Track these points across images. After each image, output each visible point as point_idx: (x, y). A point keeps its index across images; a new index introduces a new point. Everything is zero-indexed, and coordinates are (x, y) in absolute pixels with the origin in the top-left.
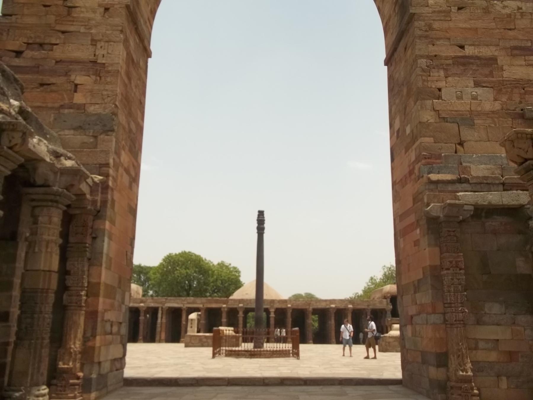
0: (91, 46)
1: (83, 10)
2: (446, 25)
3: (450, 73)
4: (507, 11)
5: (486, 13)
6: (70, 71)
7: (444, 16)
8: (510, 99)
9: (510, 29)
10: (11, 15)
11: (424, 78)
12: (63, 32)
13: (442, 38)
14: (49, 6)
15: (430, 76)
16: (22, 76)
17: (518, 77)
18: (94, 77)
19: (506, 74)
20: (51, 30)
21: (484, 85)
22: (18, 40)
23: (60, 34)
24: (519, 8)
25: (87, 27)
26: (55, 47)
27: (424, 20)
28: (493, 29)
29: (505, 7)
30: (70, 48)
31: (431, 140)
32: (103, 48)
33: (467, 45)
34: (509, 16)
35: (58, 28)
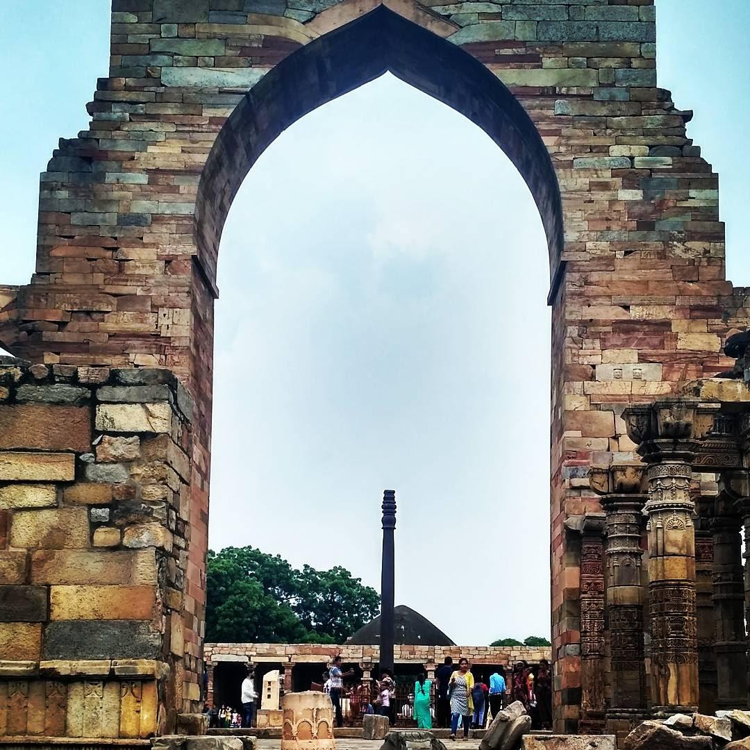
0: (151, 315)
1: (137, 264)
2: (606, 276)
3: (607, 344)
4: (690, 255)
5: (661, 258)
6: (127, 348)
7: (604, 264)
8: (683, 379)
9: (692, 282)
10: (49, 274)
11: (574, 351)
12: (115, 295)
13: (601, 296)
14: (95, 260)
15: (582, 348)
16: (70, 356)
17: (696, 348)
18: (158, 356)
19: (680, 345)
20: (100, 293)
21: (651, 360)
22: (58, 308)
23: (111, 298)
24: (706, 252)
25: (145, 288)
26: (106, 315)
27: (579, 271)
28: (670, 282)
29: (687, 250)
30: (125, 318)
31: (579, 433)
32: (167, 316)
33: (633, 305)
34: (692, 262)
35: (109, 289)
